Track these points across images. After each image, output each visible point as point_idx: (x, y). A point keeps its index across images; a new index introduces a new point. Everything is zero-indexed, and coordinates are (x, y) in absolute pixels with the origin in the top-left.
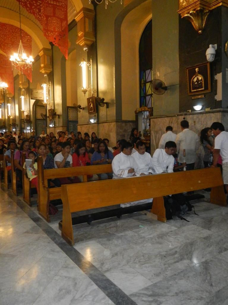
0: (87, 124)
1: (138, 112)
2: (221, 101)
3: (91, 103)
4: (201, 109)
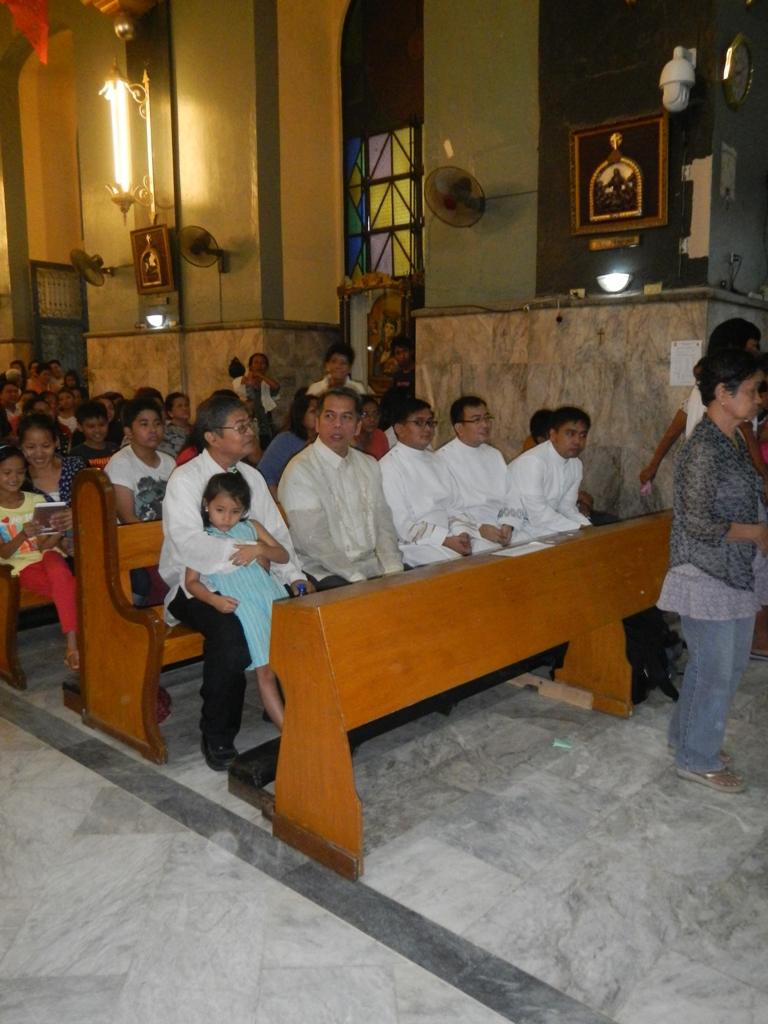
0: (133, 334)
2: (704, 261)
4: (628, 288)
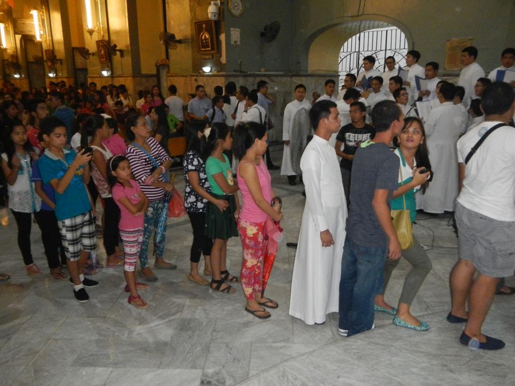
1: (158, 65)
2: (225, 64)
3: (101, 48)
4: (211, 71)
